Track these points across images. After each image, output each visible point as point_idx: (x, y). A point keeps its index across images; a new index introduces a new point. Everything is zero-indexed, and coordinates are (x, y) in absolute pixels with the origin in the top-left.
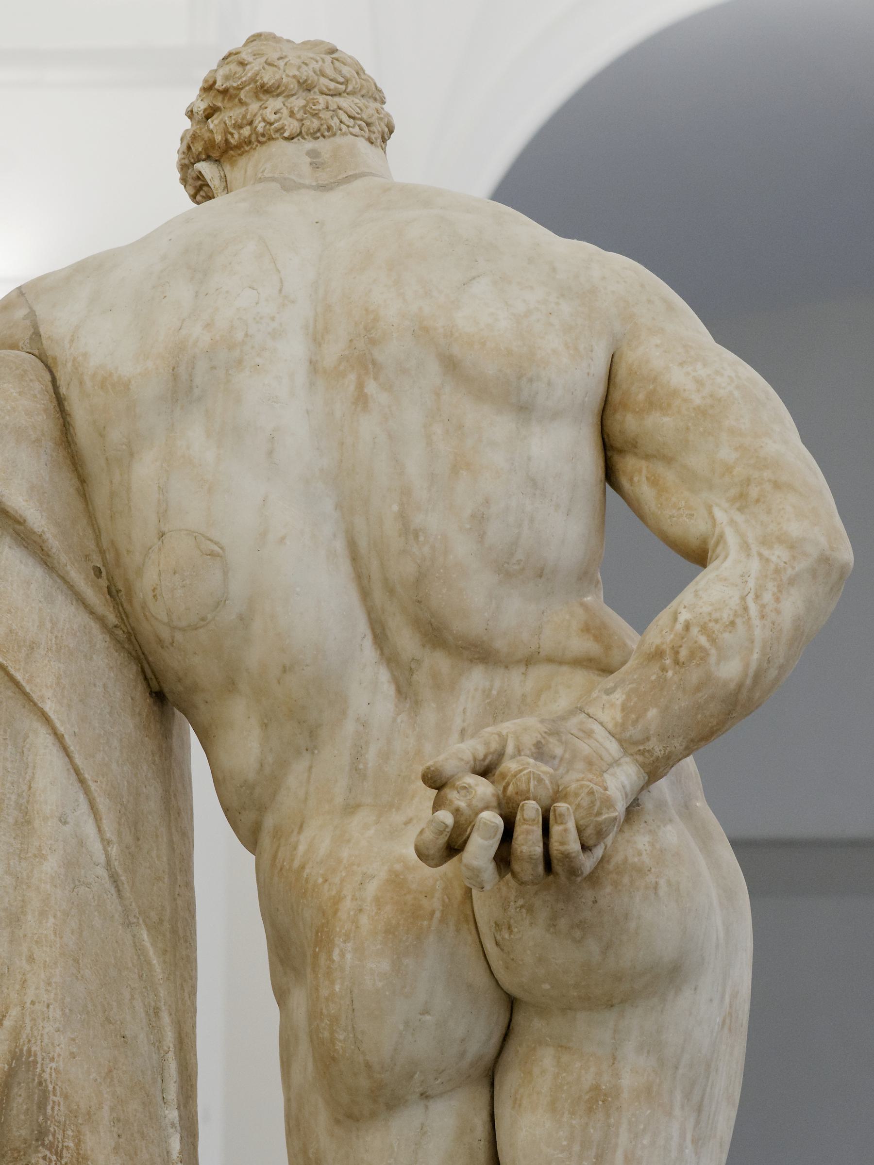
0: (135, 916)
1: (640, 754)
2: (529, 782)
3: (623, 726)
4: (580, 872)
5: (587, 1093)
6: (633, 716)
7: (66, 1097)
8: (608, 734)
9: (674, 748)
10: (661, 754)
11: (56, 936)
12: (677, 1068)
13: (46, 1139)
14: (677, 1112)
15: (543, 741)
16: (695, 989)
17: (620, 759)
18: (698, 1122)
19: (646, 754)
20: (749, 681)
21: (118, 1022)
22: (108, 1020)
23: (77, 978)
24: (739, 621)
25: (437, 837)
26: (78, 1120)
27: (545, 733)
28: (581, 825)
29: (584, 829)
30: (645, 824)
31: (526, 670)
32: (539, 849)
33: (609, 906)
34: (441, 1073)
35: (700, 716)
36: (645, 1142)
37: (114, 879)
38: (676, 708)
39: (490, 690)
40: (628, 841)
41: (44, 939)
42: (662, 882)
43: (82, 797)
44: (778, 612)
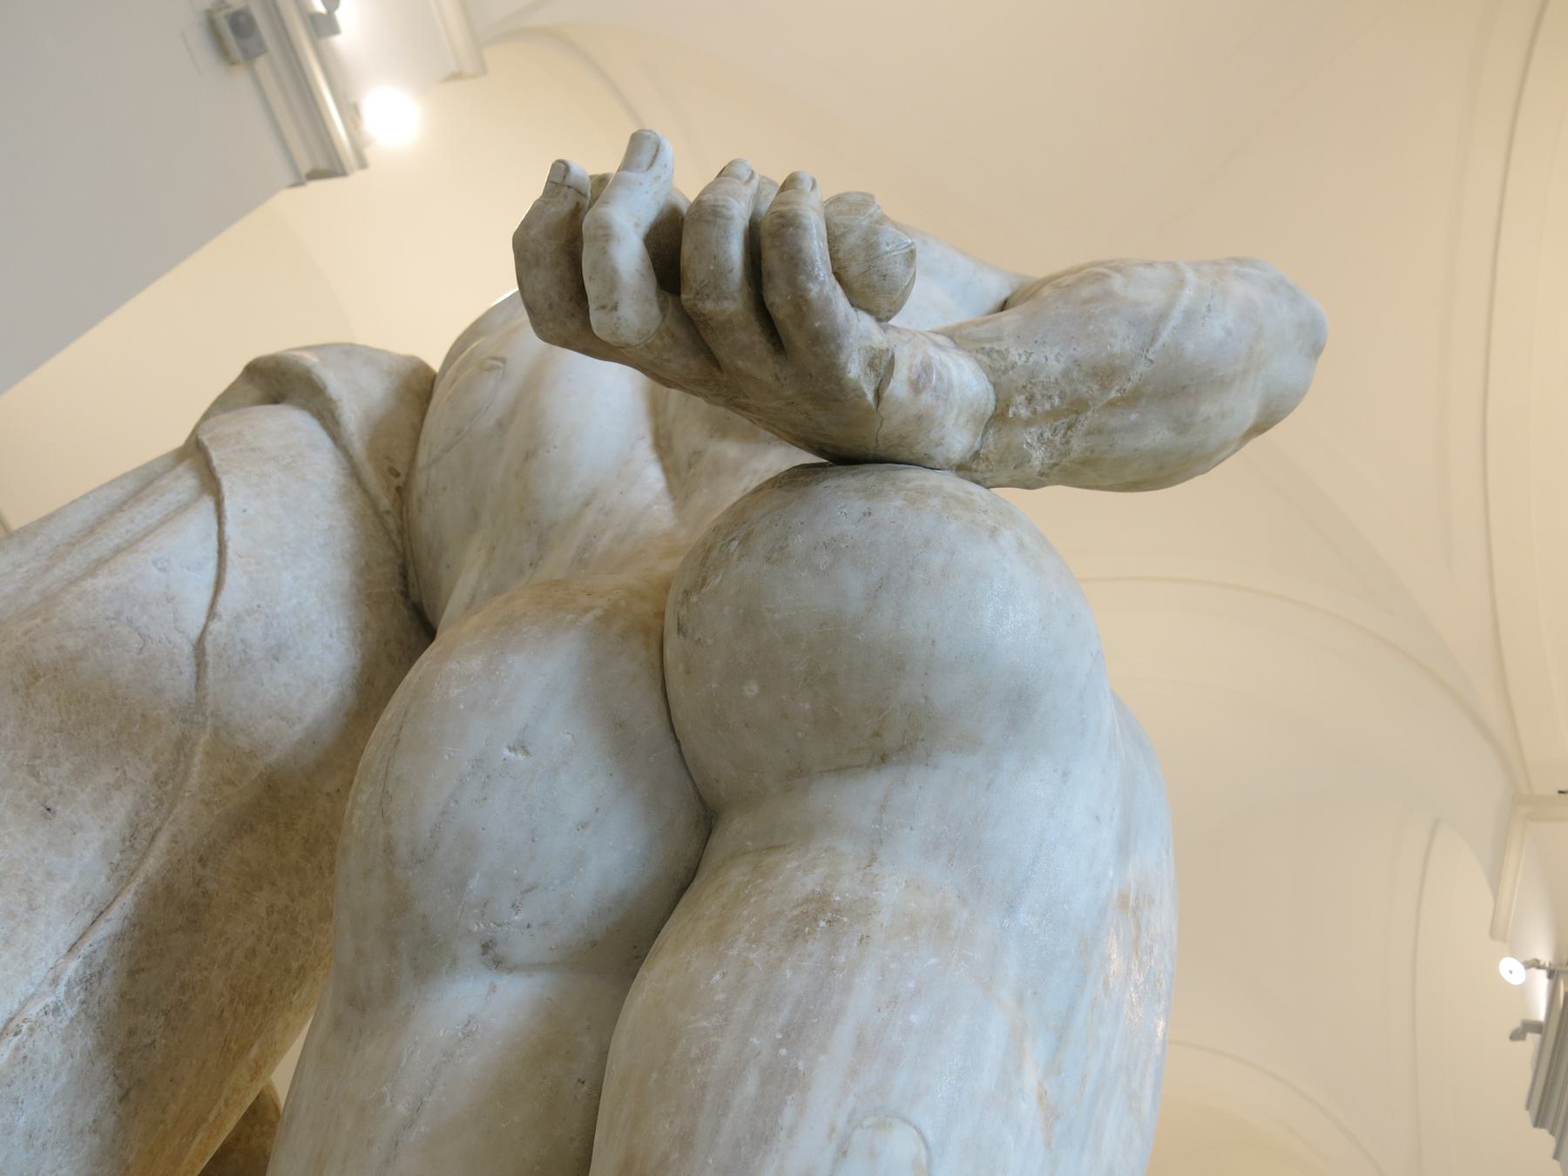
1: (983, 354)
5: (798, 905)
9: (1044, 359)
16: (1065, 774)
19: (995, 355)
23: (15, 690)
28: (836, 224)
29: (843, 235)
34: (527, 891)
35: (1091, 327)
36: (914, 1018)
43: (212, 565)
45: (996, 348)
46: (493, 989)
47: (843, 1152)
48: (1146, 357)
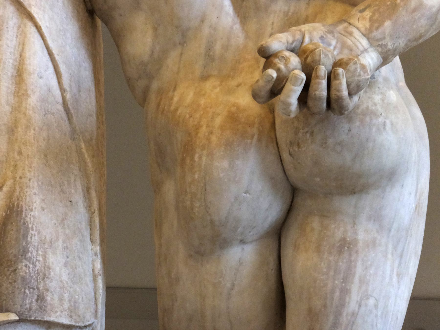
0: (78, 134)
2: (320, 56)
3: (370, 30)
4: (347, 108)
5: (339, 242)
6: (376, 25)
8: (361, 34)
10: (391, 46)
11: (34, 141)
12: (390, 231)
13: (27, 255)
14: (389, 256)
15: (324, 36)
16: (402, 186)
17: (368, 49)
18: (400, 264)
19: (383, 47)
21: (68, 193)
23: (46, 165)
25: (266, 84)
26: (45, 246)
27: (326, 32)
28: (349, 82)
30: (379, 89)
31: (309, 2)
32: (325, 93)
33: (358, 133)
36: (371, 272)
38: (402, 20)
39: (288, 12)
40: (369, 98)
41: (28, 142)
42: (388, 122)
45: (384, 43)
46: (243, 249)
47: (360, 306)
48: (432, 28)
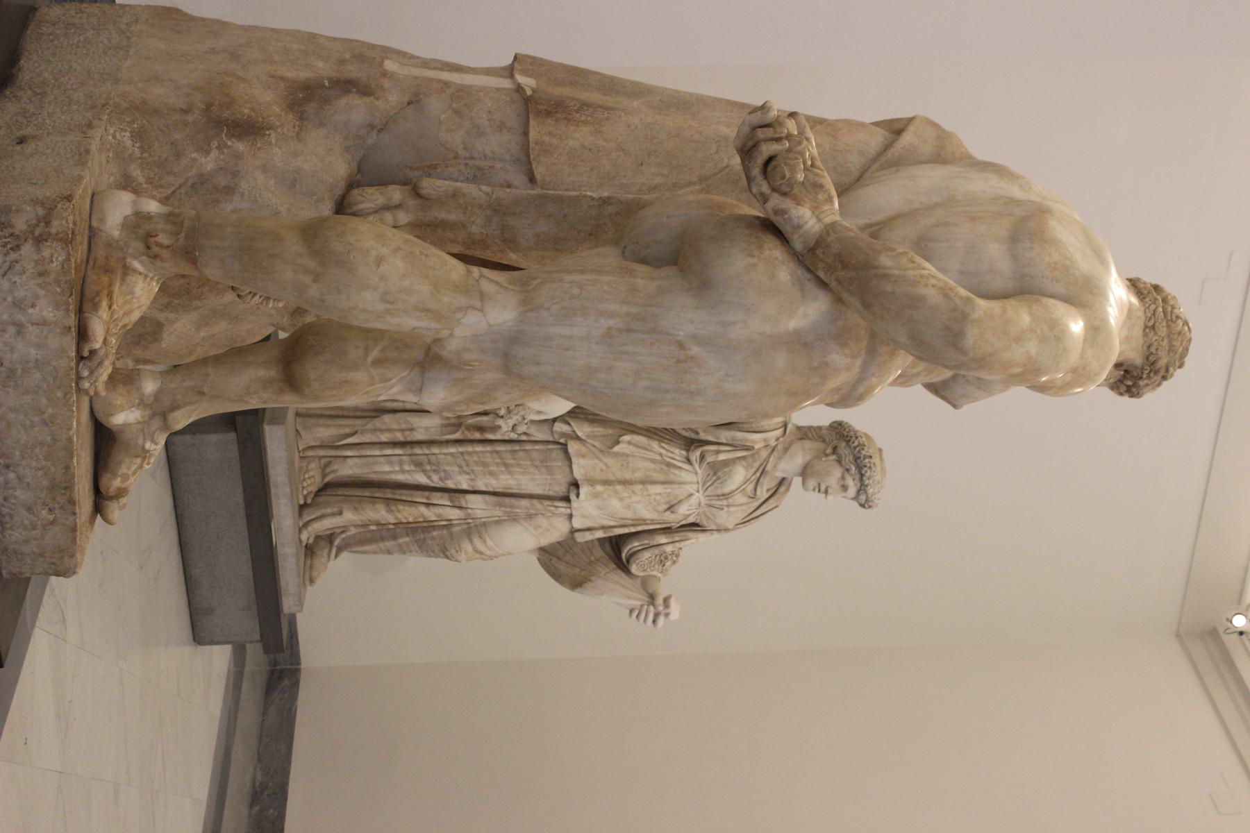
7: (608, 119)
14: (625, 309)
15: (824, 189)
16: (697, 308)
18: (620, 331)
20: (884, 271)
22: (649, 154)
24: (914, 265)
36: (605, 287)
37: (724, 169)
42: (754, 260)
44: (926, 285)
47: (569, 283)
